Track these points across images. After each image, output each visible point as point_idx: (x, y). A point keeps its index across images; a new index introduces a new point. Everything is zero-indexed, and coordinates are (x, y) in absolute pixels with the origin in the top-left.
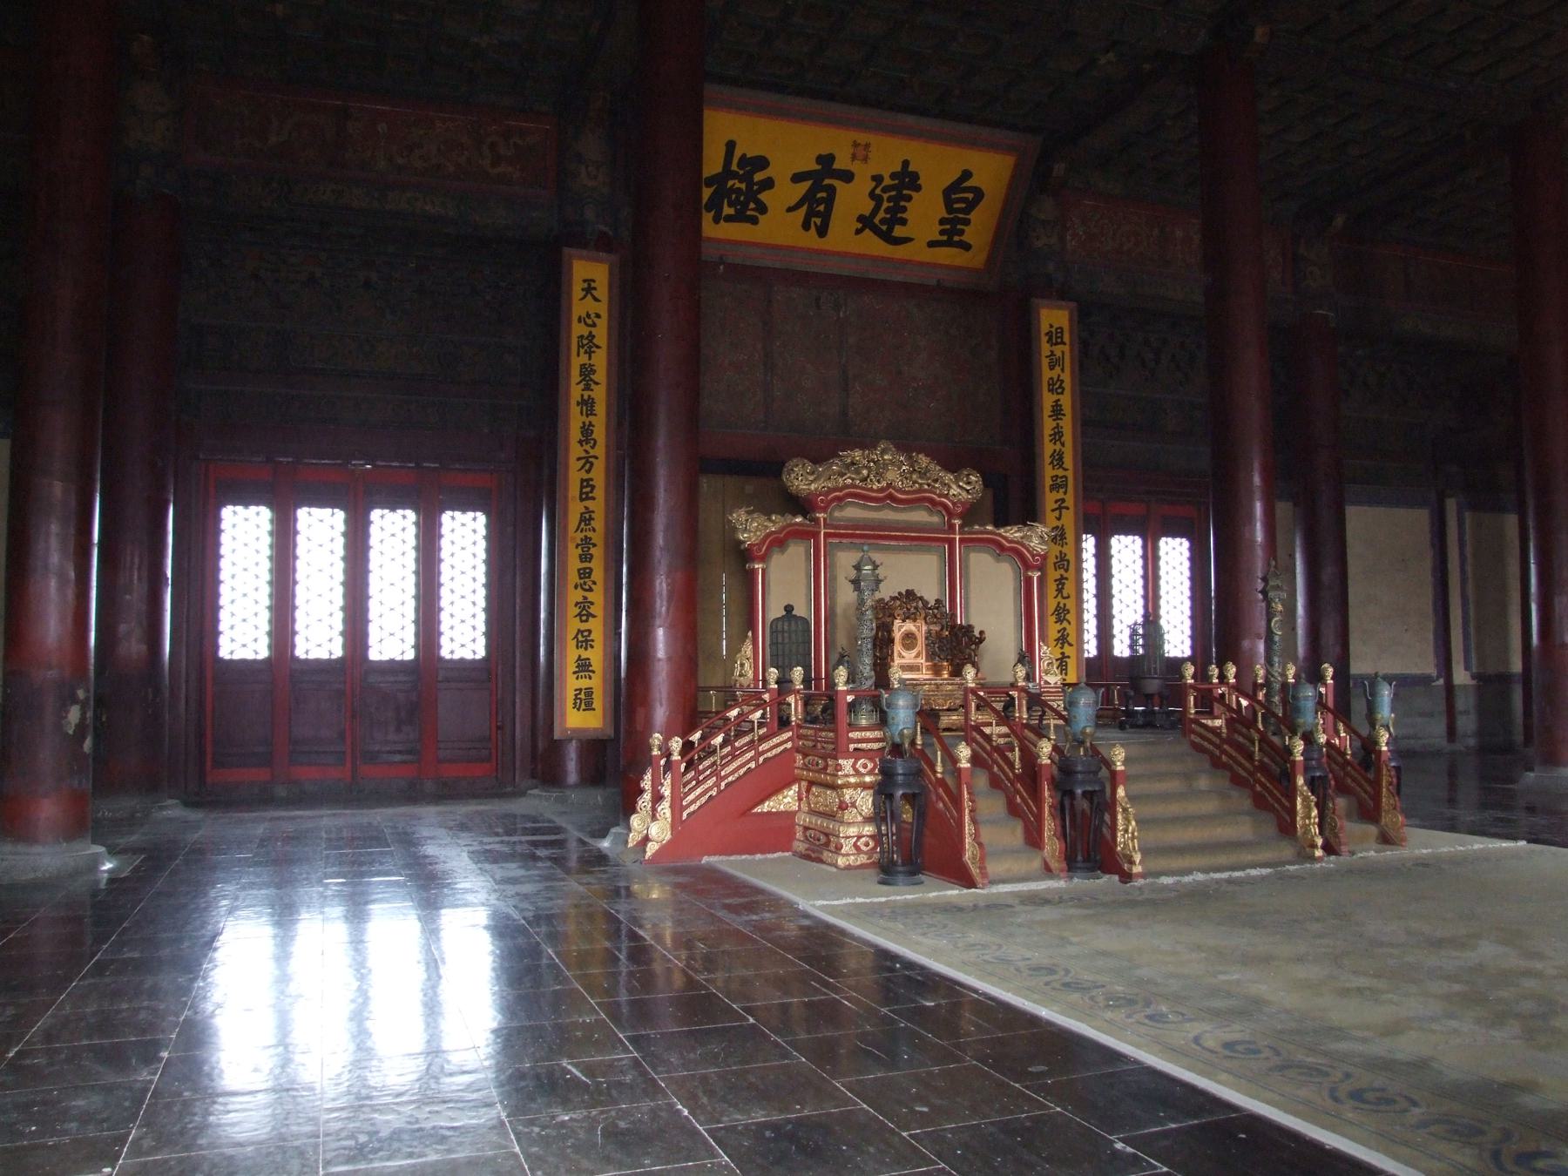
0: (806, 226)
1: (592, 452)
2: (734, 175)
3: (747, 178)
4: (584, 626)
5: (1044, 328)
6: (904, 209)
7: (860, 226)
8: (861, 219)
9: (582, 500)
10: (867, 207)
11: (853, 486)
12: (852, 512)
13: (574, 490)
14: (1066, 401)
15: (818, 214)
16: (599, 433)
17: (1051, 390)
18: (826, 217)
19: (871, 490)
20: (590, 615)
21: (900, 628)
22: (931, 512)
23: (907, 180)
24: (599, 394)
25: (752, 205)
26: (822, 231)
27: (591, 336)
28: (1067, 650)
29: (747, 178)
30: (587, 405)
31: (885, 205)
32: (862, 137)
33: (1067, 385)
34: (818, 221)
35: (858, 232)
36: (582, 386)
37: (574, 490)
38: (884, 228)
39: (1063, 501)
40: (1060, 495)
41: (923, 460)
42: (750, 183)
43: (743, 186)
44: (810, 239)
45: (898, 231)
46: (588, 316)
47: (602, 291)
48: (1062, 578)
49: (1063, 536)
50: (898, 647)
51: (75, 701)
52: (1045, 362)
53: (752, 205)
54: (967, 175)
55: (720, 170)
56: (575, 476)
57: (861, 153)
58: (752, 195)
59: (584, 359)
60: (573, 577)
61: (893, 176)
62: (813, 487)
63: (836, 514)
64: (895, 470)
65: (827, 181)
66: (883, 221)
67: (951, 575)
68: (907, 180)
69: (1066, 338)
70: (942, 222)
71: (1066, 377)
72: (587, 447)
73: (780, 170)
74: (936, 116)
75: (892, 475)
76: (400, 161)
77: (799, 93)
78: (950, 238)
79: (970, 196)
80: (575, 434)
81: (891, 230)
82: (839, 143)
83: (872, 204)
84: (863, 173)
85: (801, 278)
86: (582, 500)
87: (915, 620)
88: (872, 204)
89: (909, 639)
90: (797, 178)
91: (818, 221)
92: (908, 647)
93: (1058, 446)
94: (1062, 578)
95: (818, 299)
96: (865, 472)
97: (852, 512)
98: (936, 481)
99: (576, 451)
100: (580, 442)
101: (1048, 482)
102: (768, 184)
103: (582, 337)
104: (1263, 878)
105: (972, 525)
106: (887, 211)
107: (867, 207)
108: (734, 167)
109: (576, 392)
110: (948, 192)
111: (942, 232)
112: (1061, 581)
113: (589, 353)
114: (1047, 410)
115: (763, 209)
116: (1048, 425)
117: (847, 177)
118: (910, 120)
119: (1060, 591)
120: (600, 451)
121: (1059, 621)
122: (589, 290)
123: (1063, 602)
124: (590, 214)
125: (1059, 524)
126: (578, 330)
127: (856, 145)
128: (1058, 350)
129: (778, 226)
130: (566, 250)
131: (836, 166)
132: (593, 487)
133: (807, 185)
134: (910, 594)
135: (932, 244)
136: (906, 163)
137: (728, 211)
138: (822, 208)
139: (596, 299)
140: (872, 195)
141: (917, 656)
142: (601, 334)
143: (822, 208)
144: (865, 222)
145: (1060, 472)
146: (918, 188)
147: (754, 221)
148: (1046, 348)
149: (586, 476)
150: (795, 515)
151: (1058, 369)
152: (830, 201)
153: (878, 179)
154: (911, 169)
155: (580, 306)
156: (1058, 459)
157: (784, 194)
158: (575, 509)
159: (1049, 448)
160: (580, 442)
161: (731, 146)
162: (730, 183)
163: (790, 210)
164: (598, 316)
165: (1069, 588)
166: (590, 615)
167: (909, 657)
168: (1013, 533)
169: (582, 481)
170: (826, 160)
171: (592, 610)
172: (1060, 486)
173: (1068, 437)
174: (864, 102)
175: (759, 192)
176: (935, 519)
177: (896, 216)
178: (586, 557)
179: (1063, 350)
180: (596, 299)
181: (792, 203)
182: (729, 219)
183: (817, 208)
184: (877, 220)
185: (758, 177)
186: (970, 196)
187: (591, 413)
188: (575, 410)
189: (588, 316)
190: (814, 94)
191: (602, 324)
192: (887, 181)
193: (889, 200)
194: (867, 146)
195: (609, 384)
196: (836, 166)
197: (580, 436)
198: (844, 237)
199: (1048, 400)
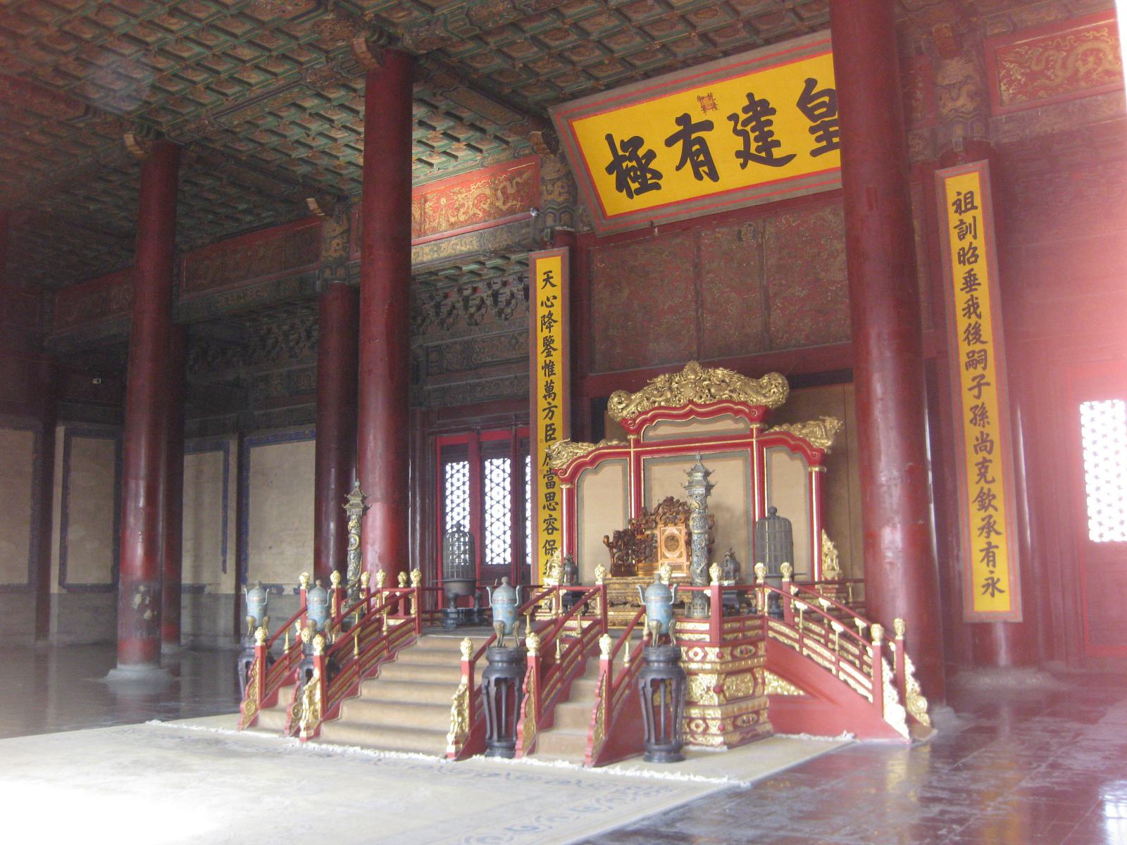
0: (699, 176)
1: (553, 403)
2: (624, 158)
3: (634, 156)
4: (550, 538)
5: (951, 197)
6: (771, 133)
7: (741, 160)
8: (738, 154)
9: (547, 441)
10: (739, 143)
11: (660, 407)
12: (665, 430)
13: (541, 434)
14: (981, 269)
15: (702, 164)
16: (558, 388)
17: (960, 262)
18: (709, 162)
19: (675, 409)
20: (554, 529)
21: (664, 531)
22: (736, 421)
23: (759, 110)
24: (557, 357)
25: (649, 176)
26: (714, 176)
27: (550, 314)
28: (994, 539)
29: (634, 156)
30: (549, 367)
31: (752, 136)
32: (703, 91)
33: (981, 251)
34: (706, 169)
35: (744, 166)
36: (545, 354)
37: (541, 434)
38: (763, 154)
39: (983, 377)
40: (979, 371)
41: (720, 372)
42: (638, 160)
43: (634, 163)
44: (707, 186)
45: (777, 153)
46: (548, 299)
47: (557, 279)
48: (985, 460)
49: (984, 415)
50: (662, 549)
51: (138, 592)
52: (954, 234)
53: (649, 176)
54: (811, 83)
55: (612, 159)
56: (542, 423)
57: (708, 103)
58: (644, 168)
59: (546, 333)
60: (542, 501)
61: (745, 110)
62: (625, 412)
63: (651, 434)
64: (688, 386)
65: (694, 136)
66: (758, 149)
67: (760, 478)
68: (759, 110)
69: (978, 201)
70: (813, 130)
71: (980, 243)
72: (550, 400)
73: (654, 141)
74: (682, 68)
75: (689, 393)
76: (453, 220)
77: (632, 80)
78: (830, 142)
79: (826, 99)
80: (541, 391)
81: (770, 154)
82: (686, 102)
83: (741, 138)
84: (718, 117)
85: (723, 218)
86: (547, 441)
87: (676, 524)
88: (741, 138)
89: (672, 538)
90: (670, 142)
91: (706, 169)
92: (669, 549)
93: (974, 319)
94: (985, 460)
95: (740, 232)
96: (669, 395)
97: (665, 430)
98: (731, 391)
99: (542, 404)
100: (545, 397)
101: (963, 359)
102: (651, 155)
103: (544, 317)
104: (430, 767)
105: (771, 427)
106: (756, 139)
107: (739, 143)
108: (620, 153)
109: (541, 359)
110: (805, 101)
111: (818, 140)
112: (983, 465)
113: (549, 327)
114: (959, 283)
115: (657, 175)
116: (961, 298)
117: (708, 126)
118: (733, 60)
119: (982, 475)
120: (558, 401)
121: (983, 507)
122: (547, 280)
123: (986, 487)
124: (550, 222)
125: (979, 402)
126: (542, 311)
127: (700, 99)
128: (968, 218)
129: (678, 186)
130: (566, 248)
131: (694, 121)
132: (554, 430)
133: (679, 145)
134: (670, 501)
135: (815, 153)
136: (750, 96)
137: (634, 186)
138: (701, 158)
139: (553, 286)
140: (736, 132)
141: (680, 556)
142: (557, 312)
143: (701, 158)
144: (745, 156)
145: (978, 347)
146: (773, 111)
147: (657, 187)
148: (954, 219)
149: (550, 422)
150: (611, 440)
151: (969, 237)
152: (704, 149)
153: (733, 117)
154: (757, 98)
155: (542, 292)
156: (974, 333)
157: (667, 158)
158: (543, 449)
159: (963, 323)
160: (545, 397)
161: (609, 138)
162: (624, 165)
163: (678, 168)
164: (555, 298)
165: (995, 470)
166: (554, 529)
167: (672, 556)
168: (797, 430)
169: (547, 426)
170: (684, 120)
171: (557, 525)
172: (978, 362)
173: (985, 307)
174: (686, 64)
175: (648, 162)
176: (741, 426)
177: (768, 143)
178: (551, 485)
179: (977, 215)
180: (553, 286)
181: (677, 162)
182: (638, 192)
183: (697, 157)
184: (753, 151)
185: (641, 152)
186: (826, 99)
187: (552, 373)
188: (541, 373)
189: (548, 299)
190: (647, 76)
191: (558, 304)
192: (743, 117)
193: (753, 130)
194: (710, 96)
195: (563, 349)
196: (694, 121)
197: (544, 393)
198: (734, 175)
199: (959, 271)
